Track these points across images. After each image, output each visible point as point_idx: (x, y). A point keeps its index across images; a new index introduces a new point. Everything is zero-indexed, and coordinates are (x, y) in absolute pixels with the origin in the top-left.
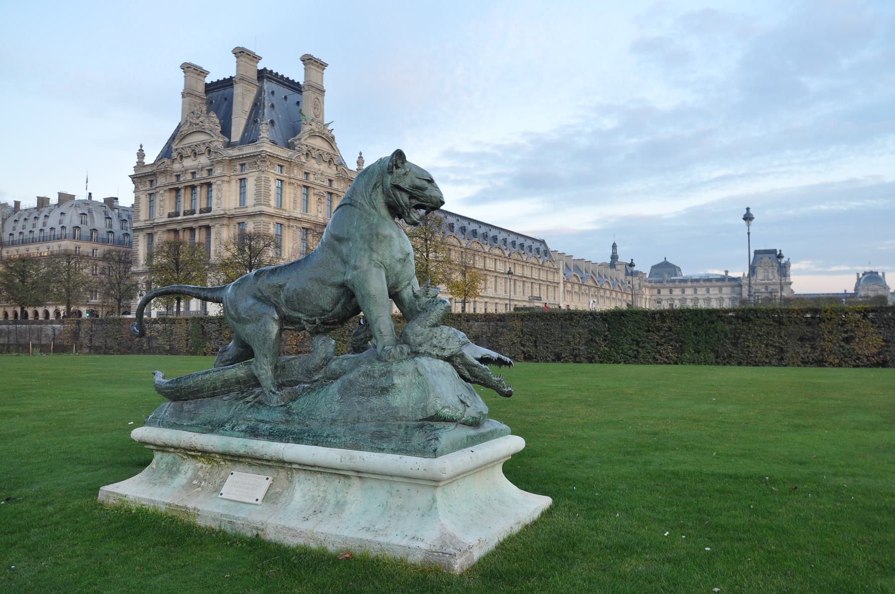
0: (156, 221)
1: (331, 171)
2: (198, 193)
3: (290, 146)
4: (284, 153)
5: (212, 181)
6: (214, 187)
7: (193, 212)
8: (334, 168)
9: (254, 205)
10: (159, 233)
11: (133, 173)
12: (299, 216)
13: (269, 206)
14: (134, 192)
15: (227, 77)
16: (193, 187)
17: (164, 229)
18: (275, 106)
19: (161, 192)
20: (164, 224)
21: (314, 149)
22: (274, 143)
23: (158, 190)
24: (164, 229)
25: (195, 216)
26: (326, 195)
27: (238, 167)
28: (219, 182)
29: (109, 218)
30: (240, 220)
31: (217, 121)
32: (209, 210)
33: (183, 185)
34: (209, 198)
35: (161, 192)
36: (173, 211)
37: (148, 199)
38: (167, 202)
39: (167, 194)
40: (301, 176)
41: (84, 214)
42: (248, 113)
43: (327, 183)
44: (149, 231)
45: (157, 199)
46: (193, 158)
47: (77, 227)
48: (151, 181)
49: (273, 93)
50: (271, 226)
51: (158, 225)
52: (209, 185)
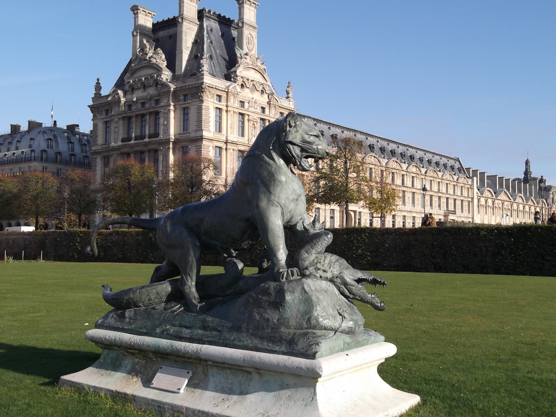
0: (113, 144)
1: (264, 99)
2: (148, 120)
3: (228, 77)
4: (222, 84)
5: (159, 110)
6: (161, 115)
7: (143, 137)
8: (266, 96)
9: (196, 131)
10: (114, 156)
11: (91, 103)
12: (235, 140)
13: (209, 131)
14: (93, 120)
15: (171, 17)
16: (143, 116)
17: (119, 152)
18: (213, 42)
19: (116, 120)
20: (118, 148)
21: (248, 80)
22: (213, 75)
23: (113, 118)
24: (119, 152)
25: (147, 140)
26: (259, 121)
27: (182, 98)
28: (165, 111)
29: (71, 143)
30: (184, 144)
31: (163, 57)
32: (156, 135)
33: (134, 114)
34: (156, 124)
35: (116, 120)
36: (126, 136)
37: (104, 126)
38: (121, 129)
39: (121, 122)
40: (237, 105)
41: (50, 139)
42: (190, 49)
43: (259, 110)
44: (105, 154)
45: (113, 126)
46: (142, 89)
47: (44, 151)
48: (107, 111)
49: (211, 30)
50: (211, 149)
51: (114, 149)
52: (157, 113)
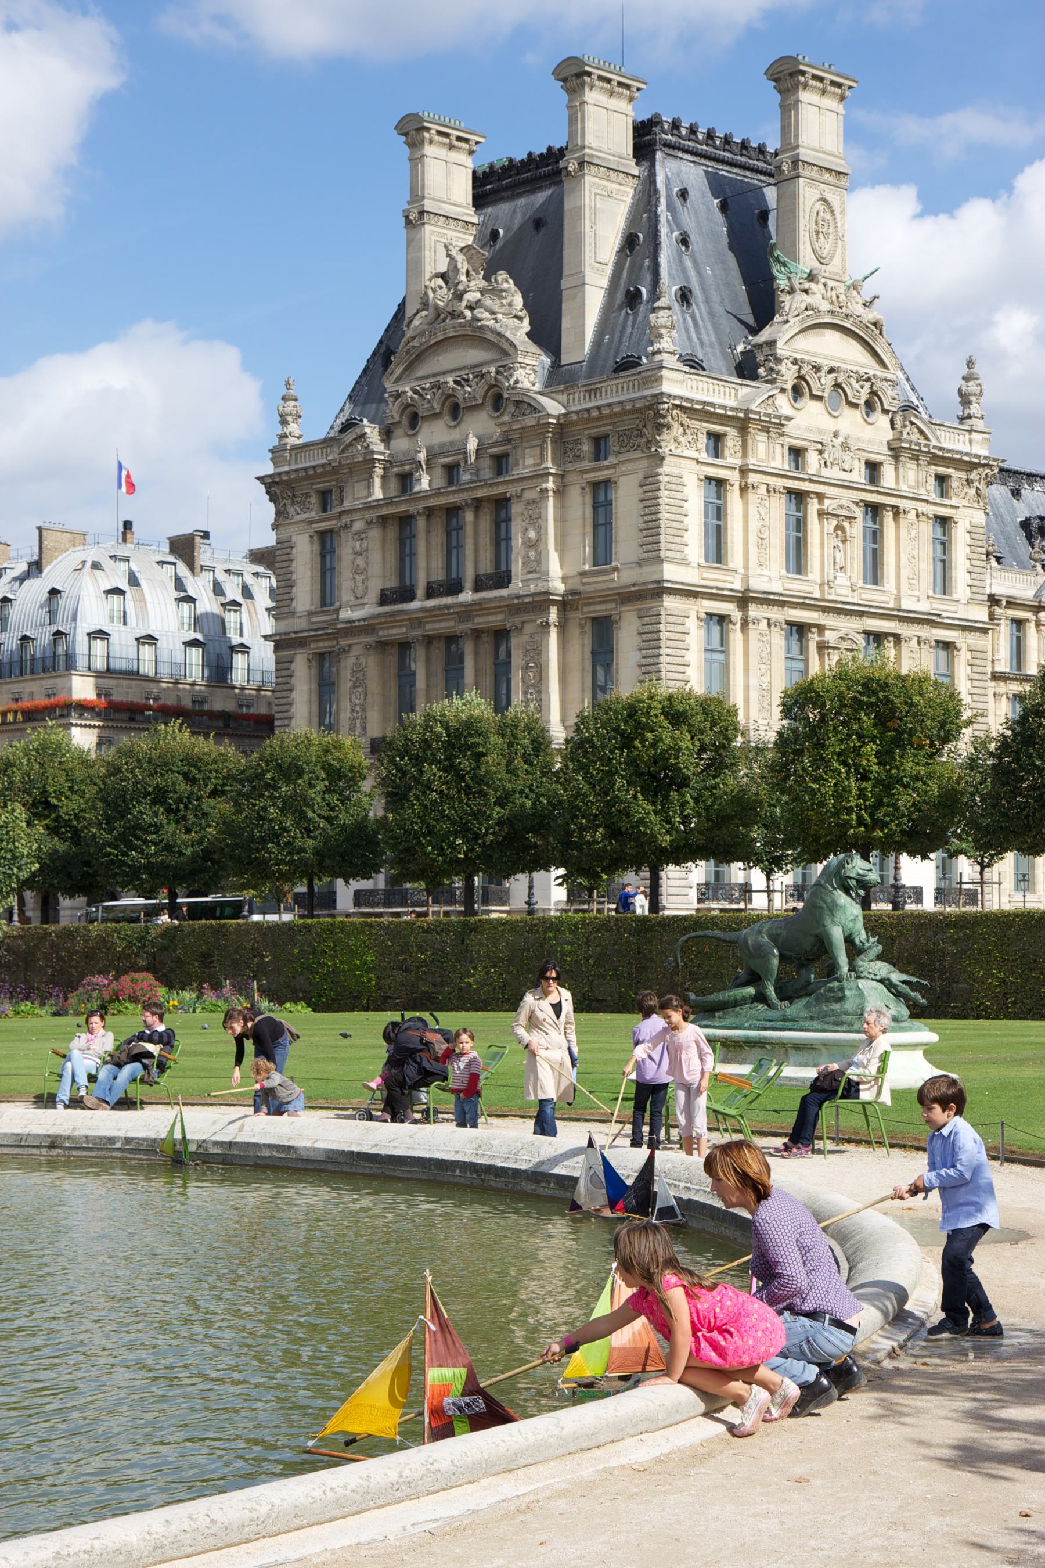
0: (346, 614)
1: (875, 434)
2: (469, 529)
3: (747, 369)
4: (725, 394)
5: (511, 490)
6: (516, 508)
7: (454, 587)
8: (884, 421)
9: (640, 563)
10: (356, 651)
11: (269, 469)
12: (776, 587)
13: (685, 563)
14: (275, 526)
15: (540, 149)
16: (452, 512)
17: (370, 639)
18: (693, 238)
19: (358, 526)
20: (366, 627)
21: (817, 369)
22: (693, 364)
23: (346, 519)
24: (370, 639)
25: (467, 596)
26: (859, 512)
27: (586, 447)
28: (529, 495)
29: (190, 600)
30: (599, 610)
31: (518, 301)
32: (502, 579)
33: (421, 505)
34: (501, 541)
35: (358, 526)
36: (393, 583)
37: (317, 547)
38: (376, 557)
39: (375, 533)
40: (781, 461)
41: (118, 591)
42: (609, 270)
43: (859, 475)
44: (323, 646)
45: (346, 550)
46: (447, 418)
47: (101, 632)
48: (325, 499)
49: (684, 194)
50: (692, 624)
51: (353, 629)
52: (502, 503)
